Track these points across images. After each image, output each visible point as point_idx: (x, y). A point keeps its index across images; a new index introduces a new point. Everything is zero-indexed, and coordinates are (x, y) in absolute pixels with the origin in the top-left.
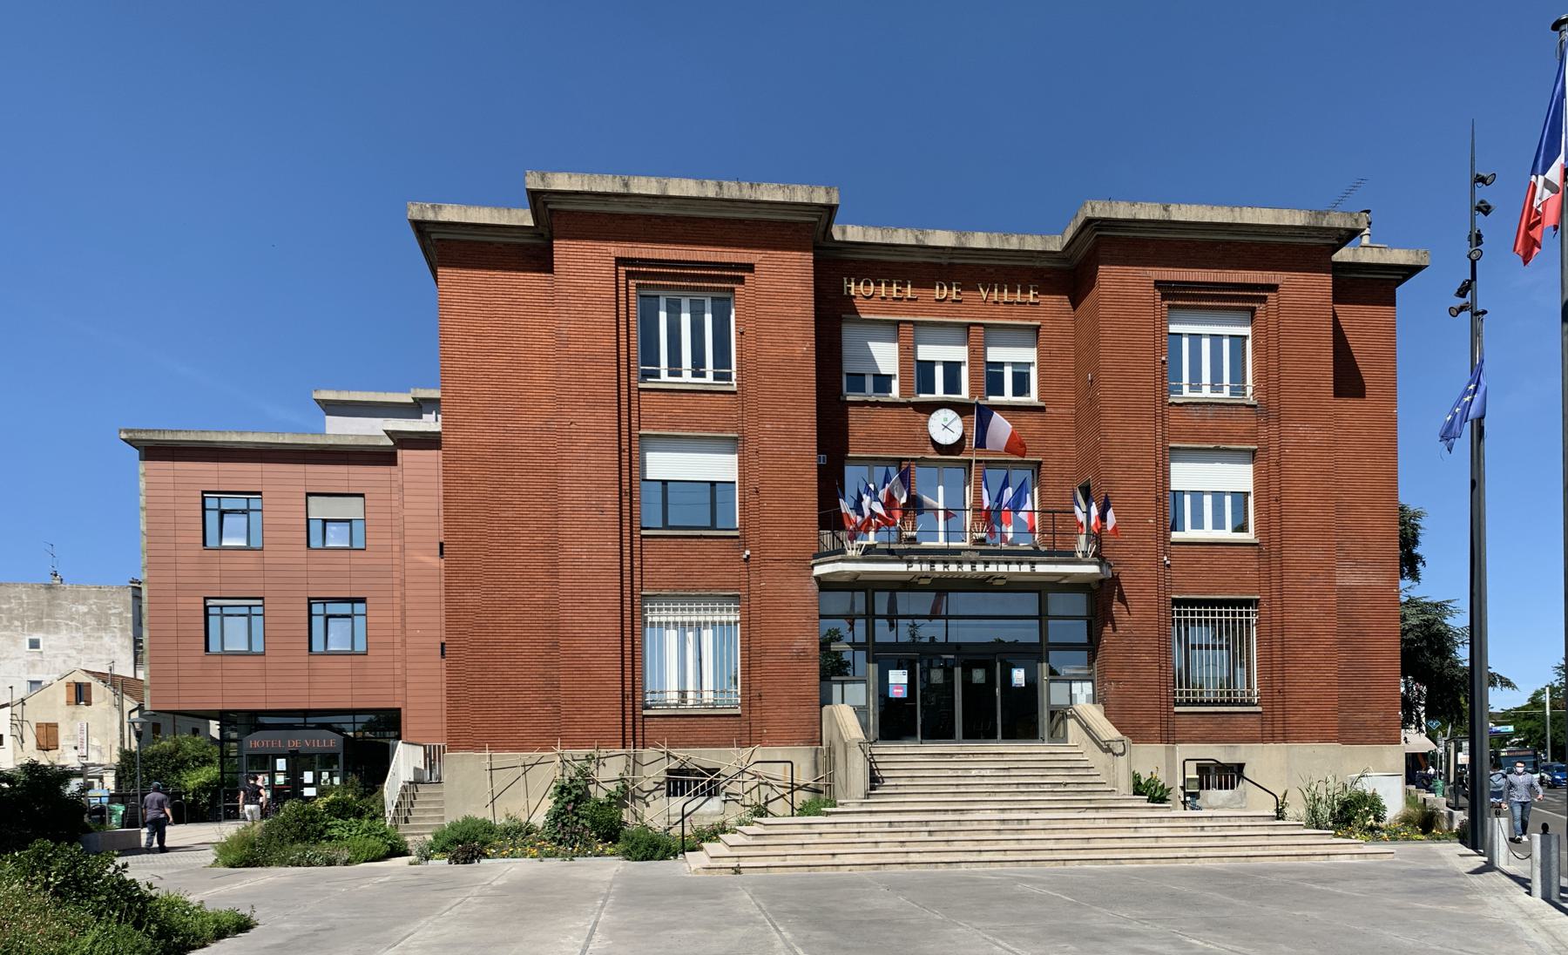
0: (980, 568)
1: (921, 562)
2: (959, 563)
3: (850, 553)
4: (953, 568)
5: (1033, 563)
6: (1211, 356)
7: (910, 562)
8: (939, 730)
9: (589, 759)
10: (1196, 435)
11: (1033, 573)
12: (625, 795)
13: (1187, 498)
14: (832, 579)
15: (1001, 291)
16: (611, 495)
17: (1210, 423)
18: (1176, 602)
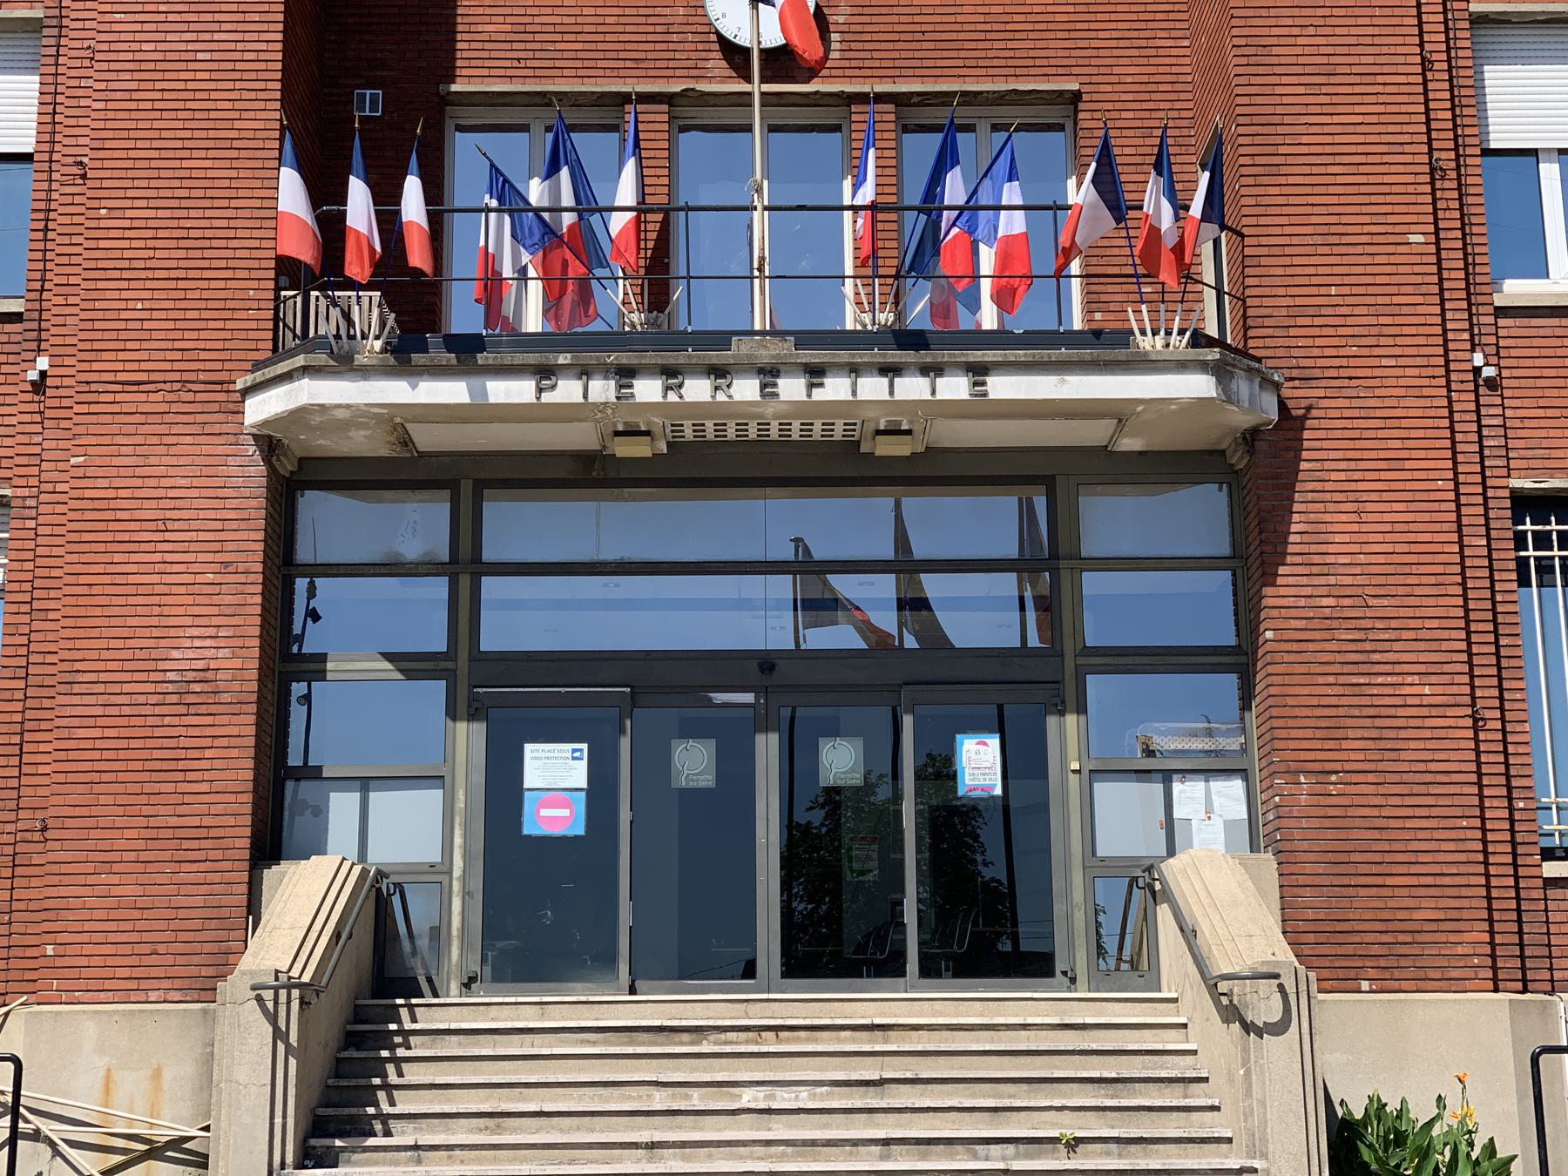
1: (585, 372)
2: (719, 372)
3: (360, 359)
5: (978, 371)
7: (545, 373)
13: (1550, 173)
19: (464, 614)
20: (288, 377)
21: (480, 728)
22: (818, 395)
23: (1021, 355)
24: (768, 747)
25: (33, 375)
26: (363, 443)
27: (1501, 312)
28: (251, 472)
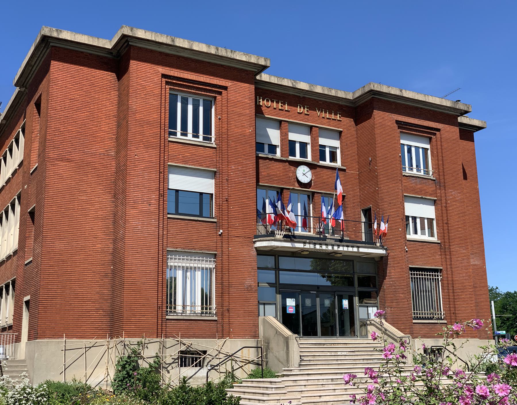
0: (336, 248)
1: (309, 243)
2: (327, 245)
4: (324, 247)
5: (358, 247)
6: (416, 156)
8: (310, 331)
9: (139, 344)
10: (414, 191)
11: (358, 252)
12: (157, 367)
14: (262, 249)
15: (326, 112)
16: (155, 196)
17: (419, 186)
18: (411, 269)
19: (277, 277)
20: (269, 240)
21: (280, 295)
23: (364, 245)
24: (318, 300)
25: (220, 233)
27: (408, 241)
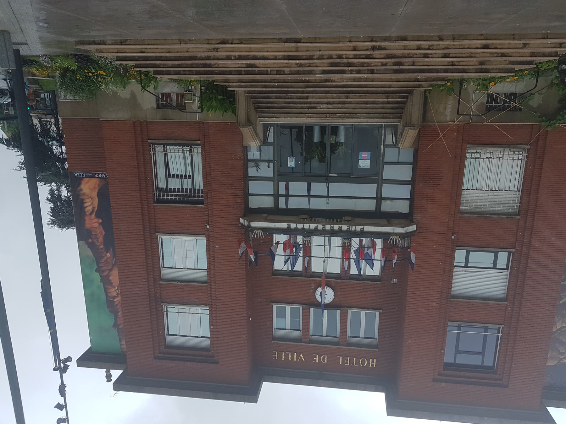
11: (289, 222)
19: (379, 191)
22: (316, 225)
25: (455, 235)
26: (396, 221)
28: (416, 217)
